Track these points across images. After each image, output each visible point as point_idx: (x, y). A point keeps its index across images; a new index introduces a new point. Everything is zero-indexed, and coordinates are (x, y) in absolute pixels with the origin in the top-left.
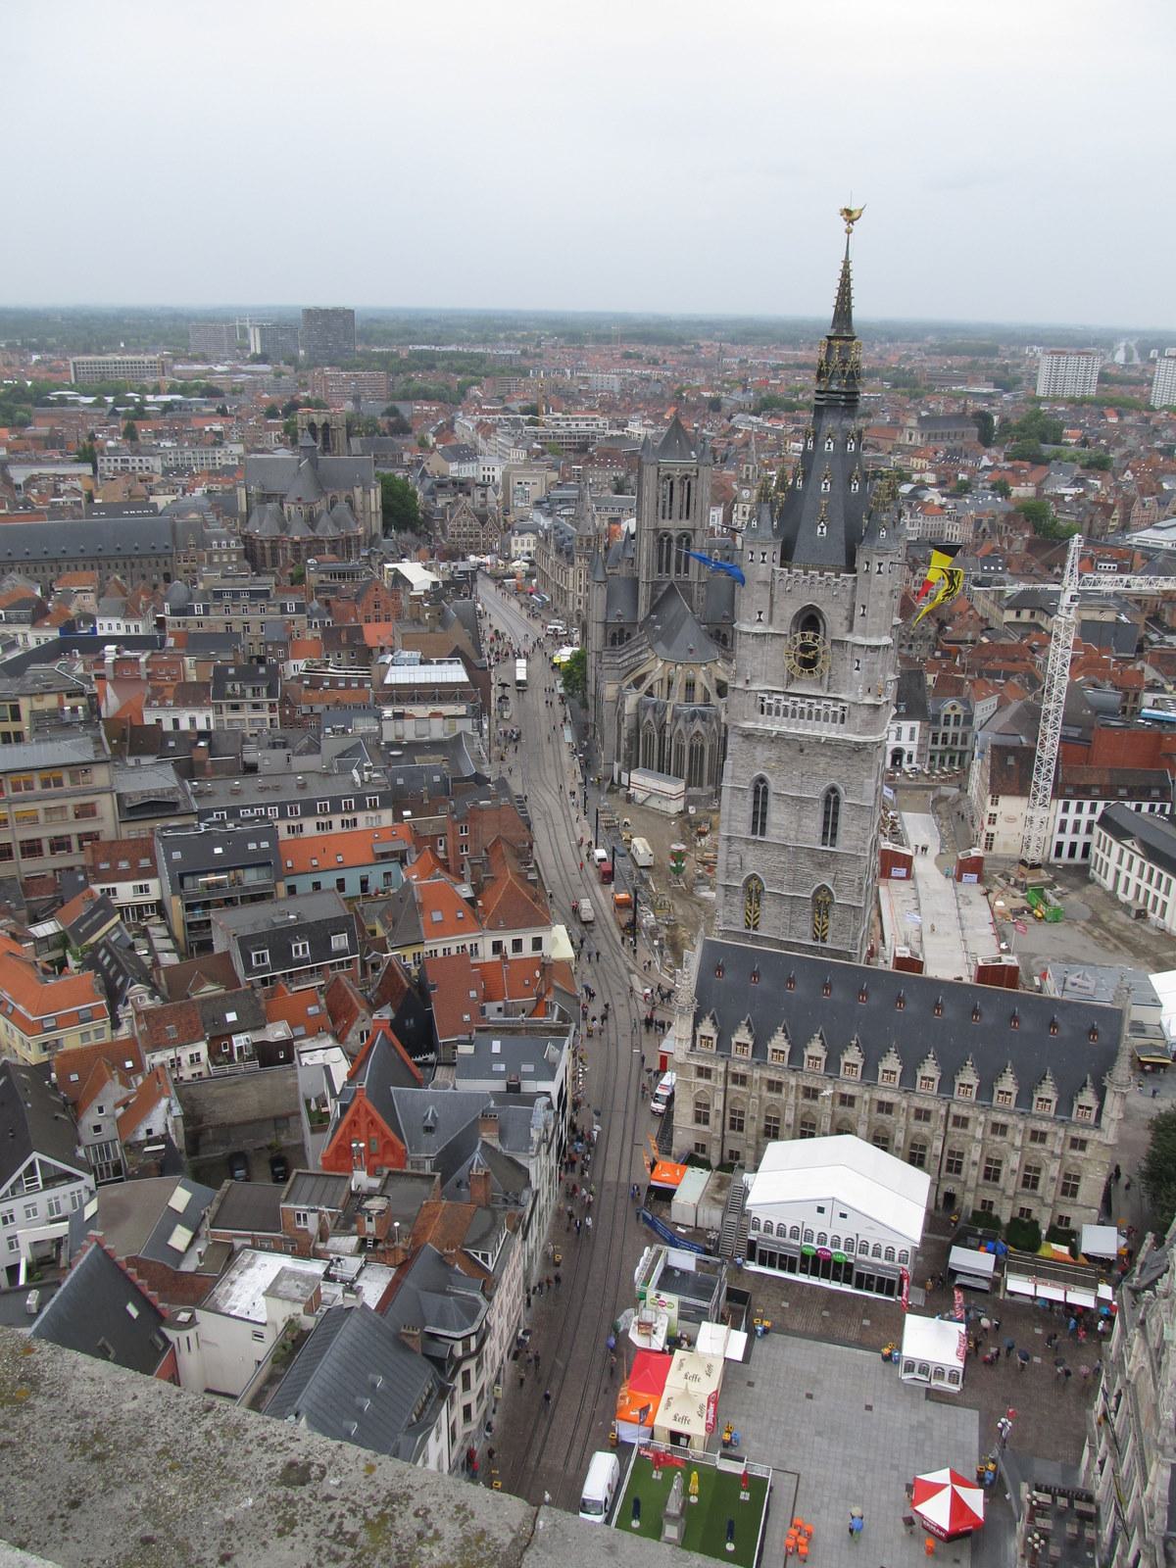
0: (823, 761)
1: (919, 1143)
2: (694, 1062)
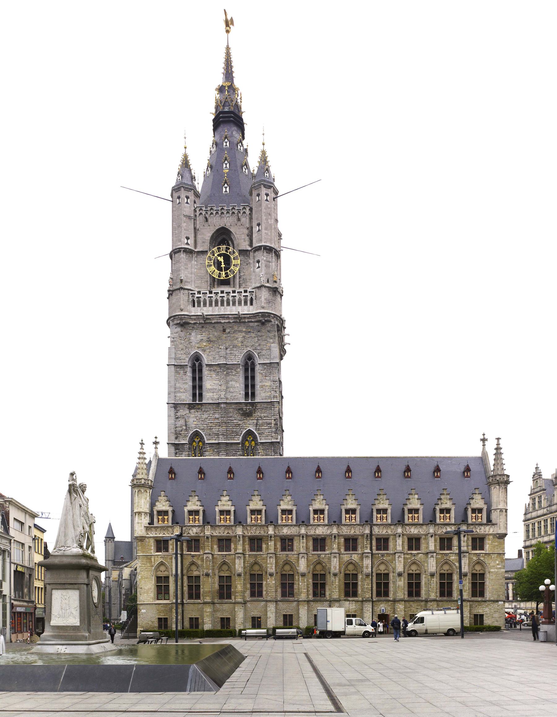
0: (240, 336)
1: (351, 572)
2: (152, 534)
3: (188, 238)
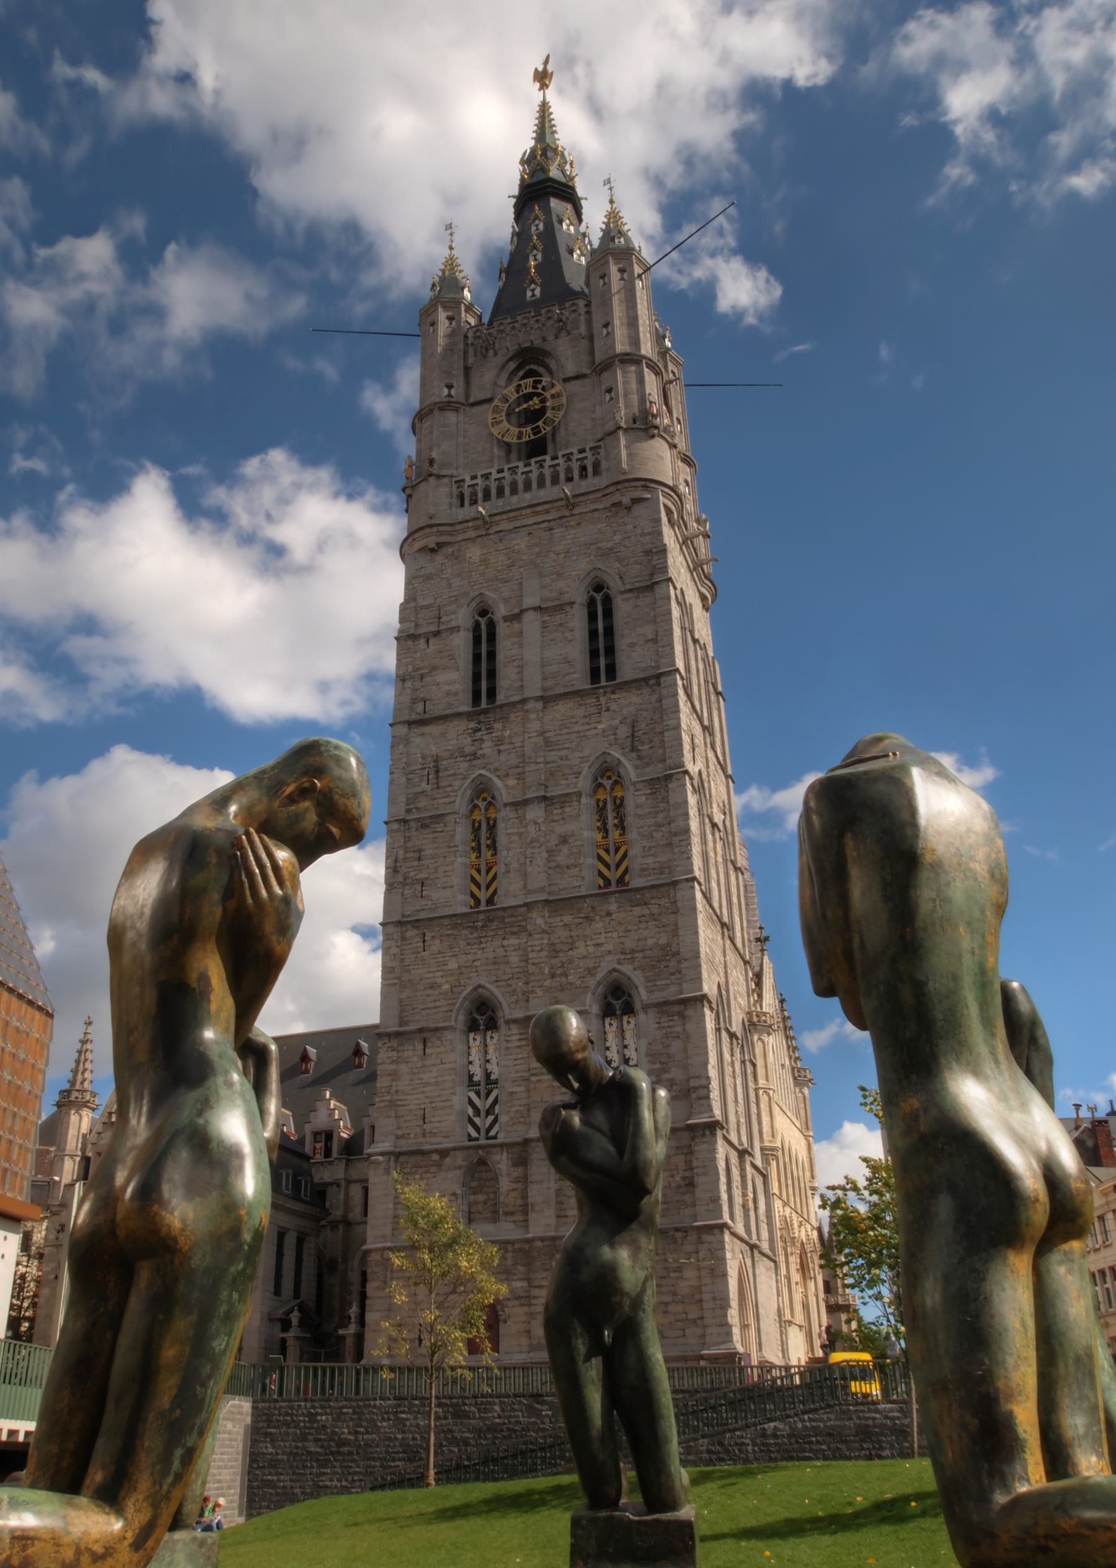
3: (450, 387)
